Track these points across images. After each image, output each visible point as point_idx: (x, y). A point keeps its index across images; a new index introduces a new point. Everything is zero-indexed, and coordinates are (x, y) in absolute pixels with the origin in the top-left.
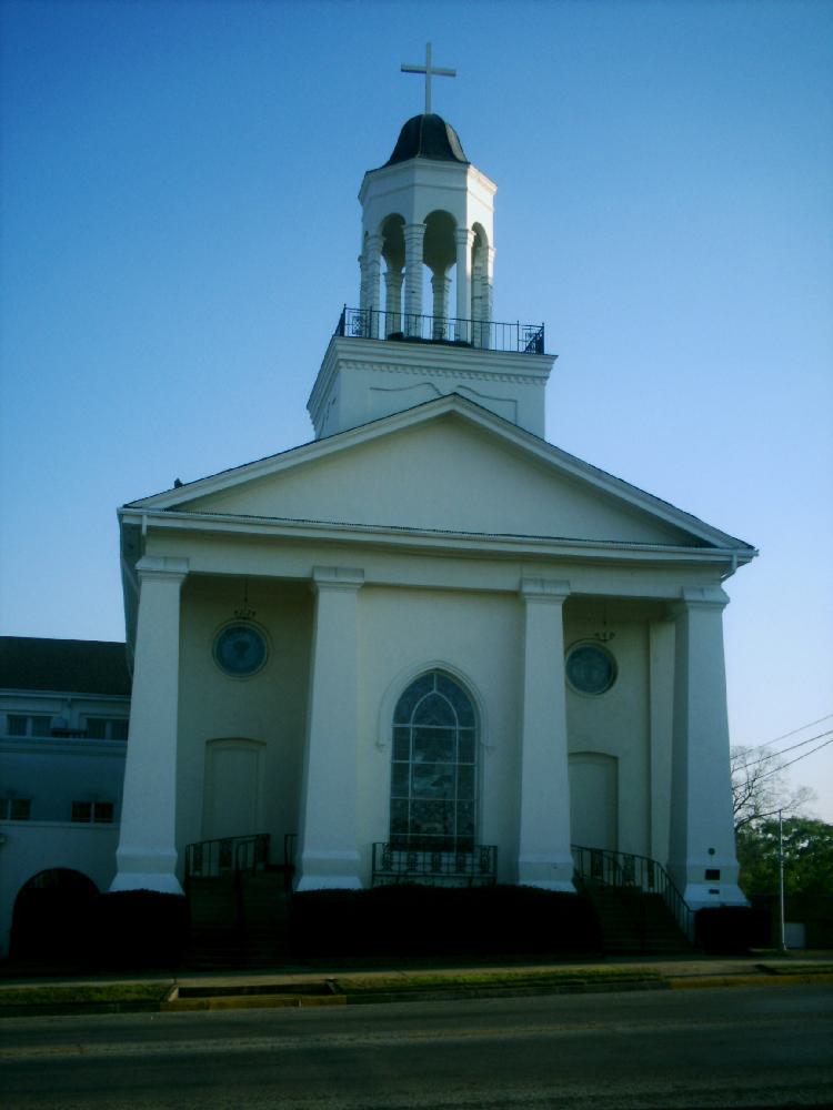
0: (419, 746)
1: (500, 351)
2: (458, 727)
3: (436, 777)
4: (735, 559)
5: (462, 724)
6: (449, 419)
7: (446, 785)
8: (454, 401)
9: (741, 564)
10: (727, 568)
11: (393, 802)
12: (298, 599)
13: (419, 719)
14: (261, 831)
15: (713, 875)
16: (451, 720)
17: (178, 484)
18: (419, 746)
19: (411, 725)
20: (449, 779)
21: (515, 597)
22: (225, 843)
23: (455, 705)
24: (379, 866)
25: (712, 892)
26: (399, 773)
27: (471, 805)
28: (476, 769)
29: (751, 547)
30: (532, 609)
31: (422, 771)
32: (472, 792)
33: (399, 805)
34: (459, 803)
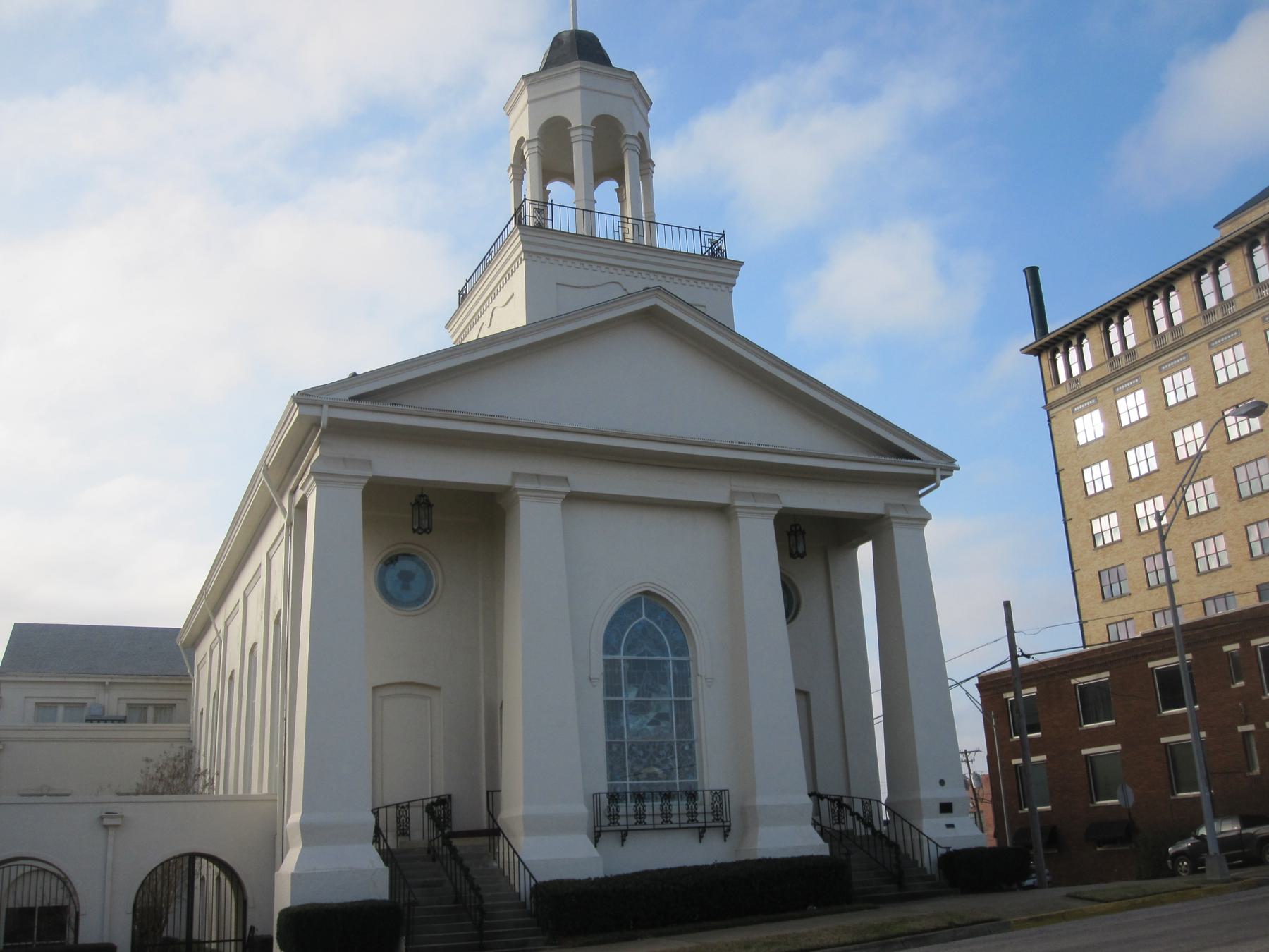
0: (631, 680)
1: (672, 252)
2: (671, 658)
3: (652, 715)
4: (939, 473)
5: (675, 654)
6: (652, 318)
7: (664, 724)
8: (657, 296)
9: (943, 477)
10: (928, 481)
11: (609, 746)
12: (481, 519)
13: (629, 649)
14: (441, 791)
15: (946, 808)
16: (665, 652)
17: (355, 374)
18: (631, 680)
19: (621, 656)
20: (665, 717)
21: (722, 511)
22: (402, 808)
23: (666, 632)
24: (605, 821)
25: (950, 826)
26: (613, 710)
27: (691, 745)
28: (693, 704)
29: (952, 460)
30: (744, 523)
31: (639, 708)
32: (690, 731)
33: (614, 749)
34: (679, 744)
